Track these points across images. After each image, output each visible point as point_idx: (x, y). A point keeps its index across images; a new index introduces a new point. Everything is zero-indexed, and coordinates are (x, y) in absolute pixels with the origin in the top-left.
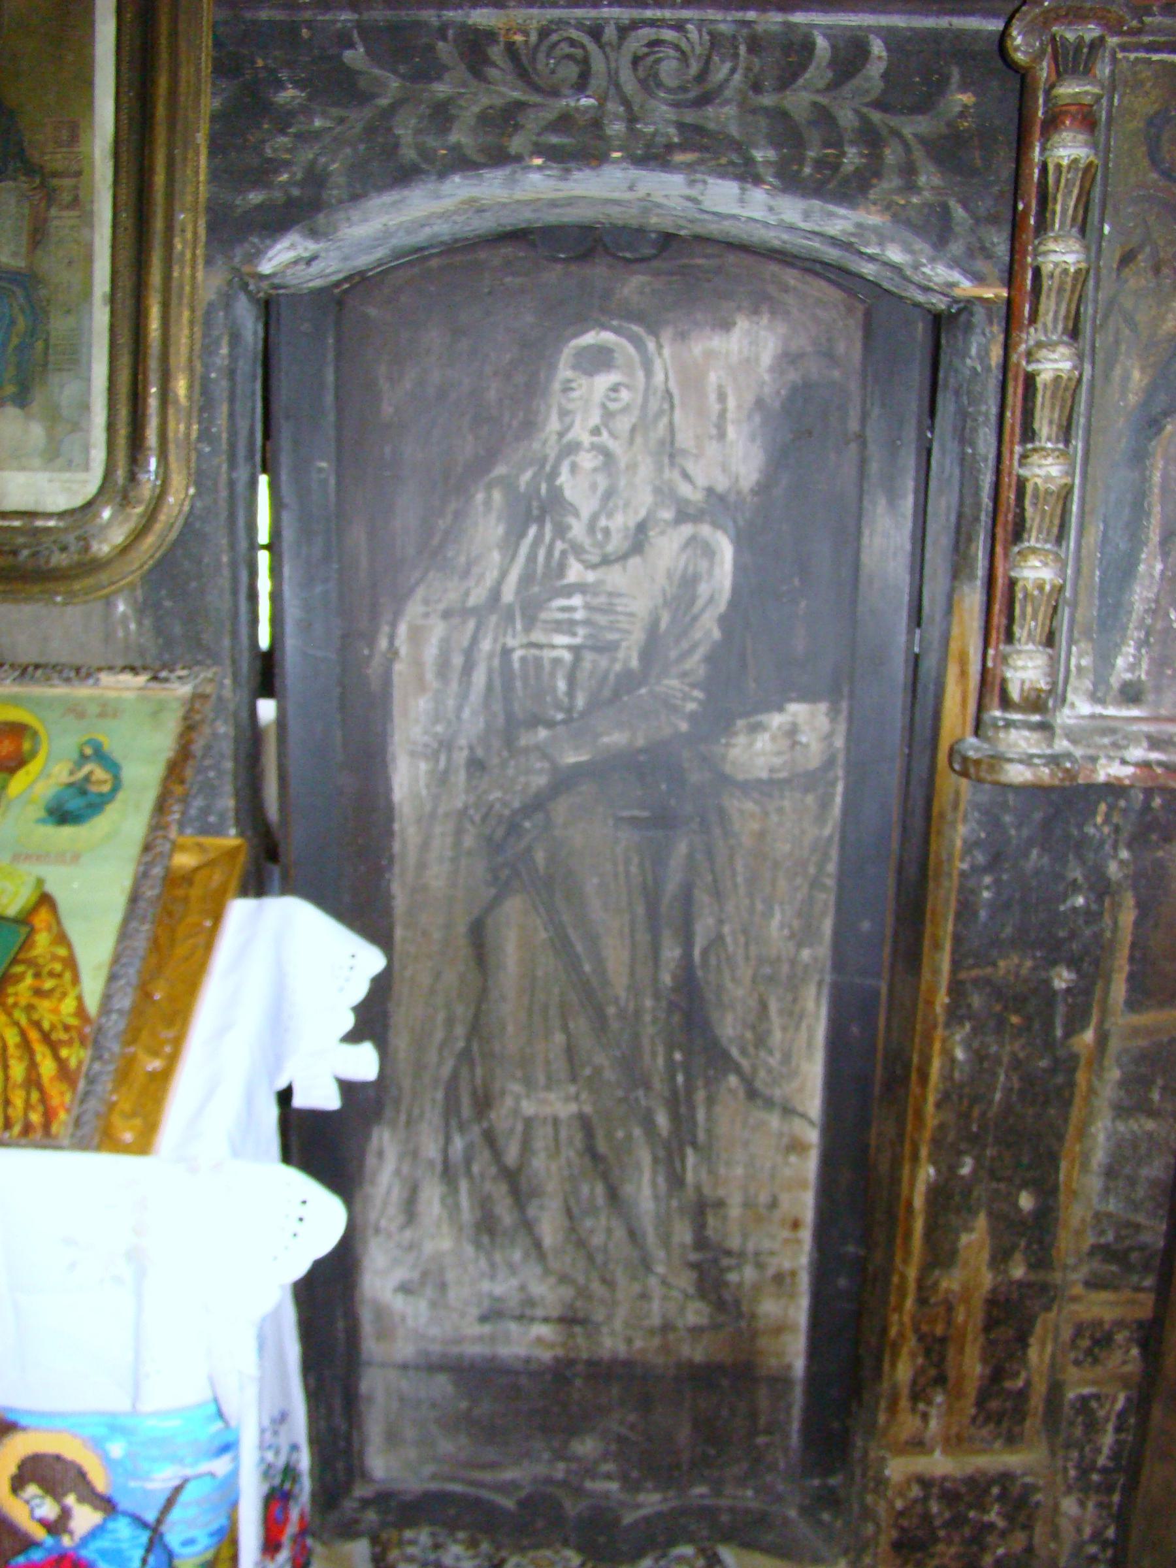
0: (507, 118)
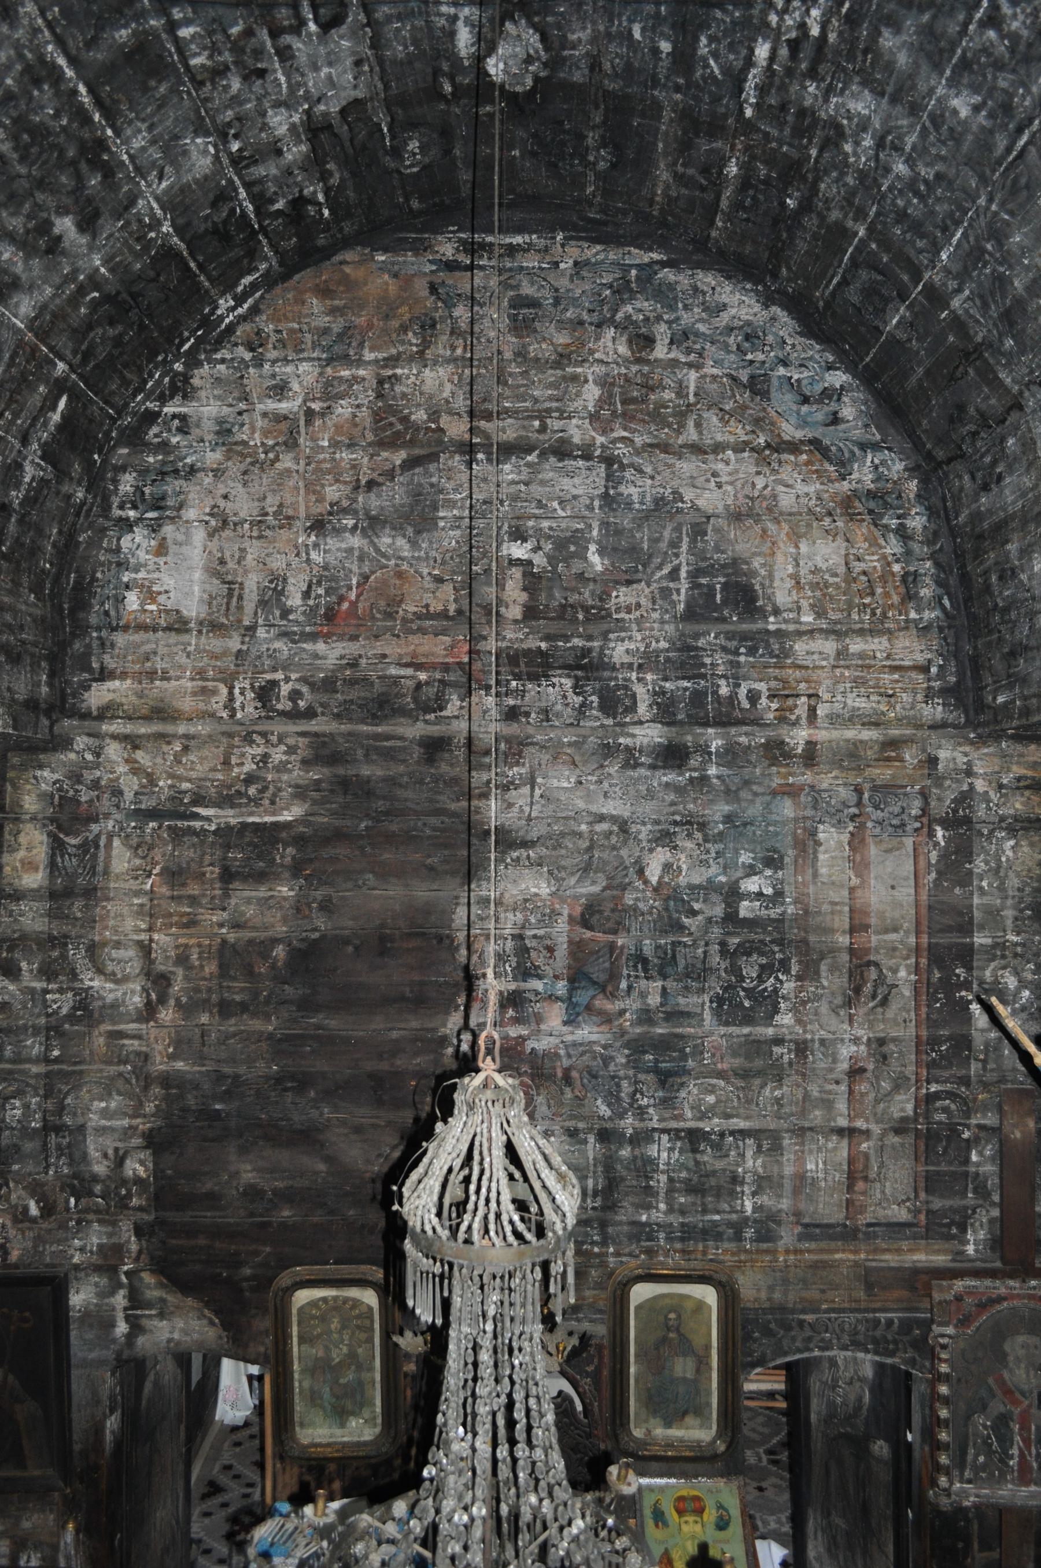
0: (809, 1339)
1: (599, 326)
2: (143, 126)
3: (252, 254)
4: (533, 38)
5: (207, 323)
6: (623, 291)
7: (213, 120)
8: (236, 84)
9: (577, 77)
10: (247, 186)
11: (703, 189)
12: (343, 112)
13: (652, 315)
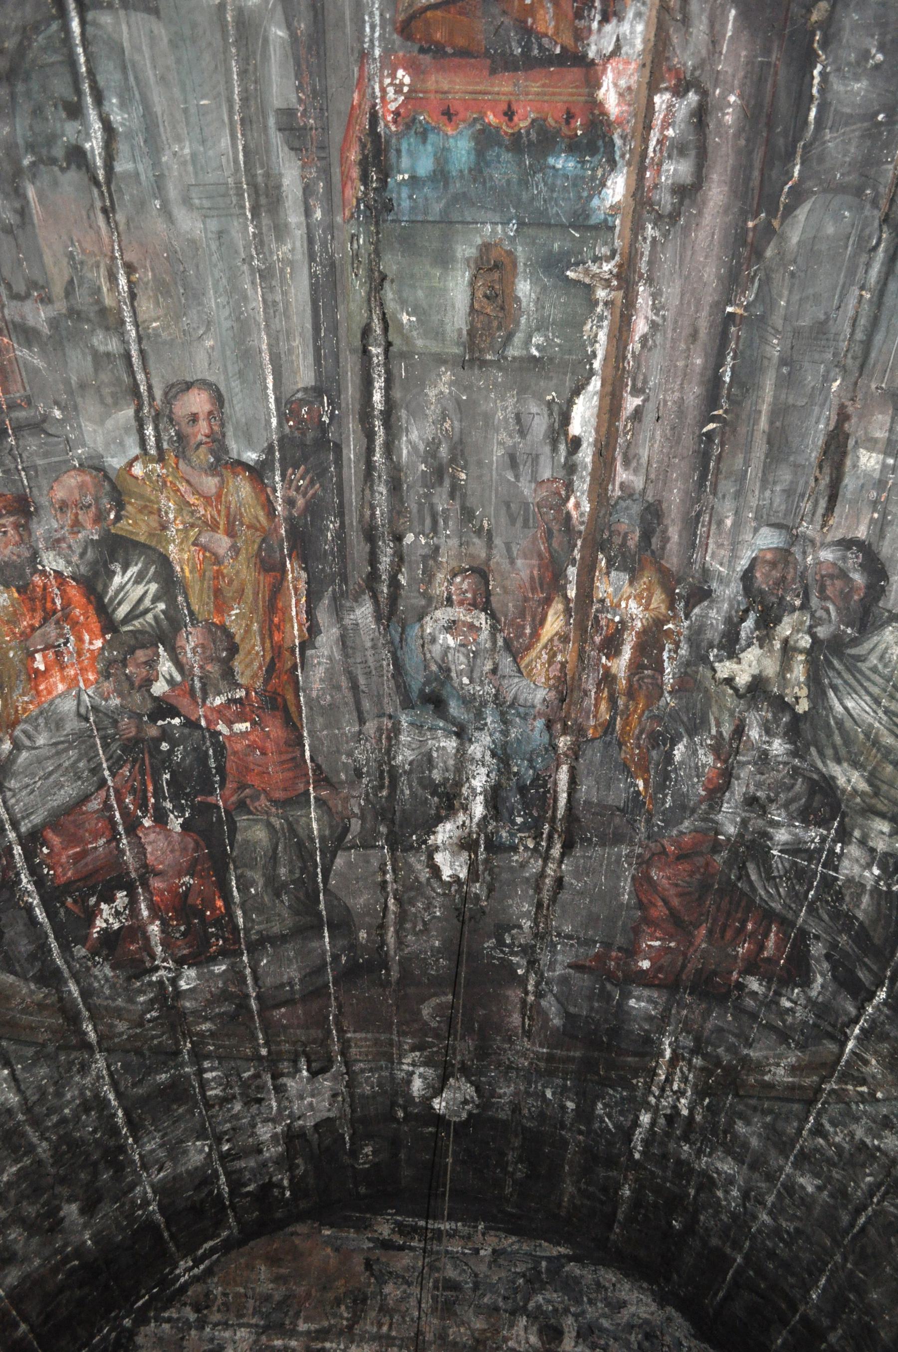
1: (513, 1313)
2: (158, 1135)
3: (219, 1223)
4: (470, 1090)
5: (164, 1283)
6: (535, 1281)
7: (213, 1130)
8: (238, 1107)
9: (502, 1115)
10: (228, 1174)
11: (602, 1203)
12: (317, 1126)
13: (560, 1307)
